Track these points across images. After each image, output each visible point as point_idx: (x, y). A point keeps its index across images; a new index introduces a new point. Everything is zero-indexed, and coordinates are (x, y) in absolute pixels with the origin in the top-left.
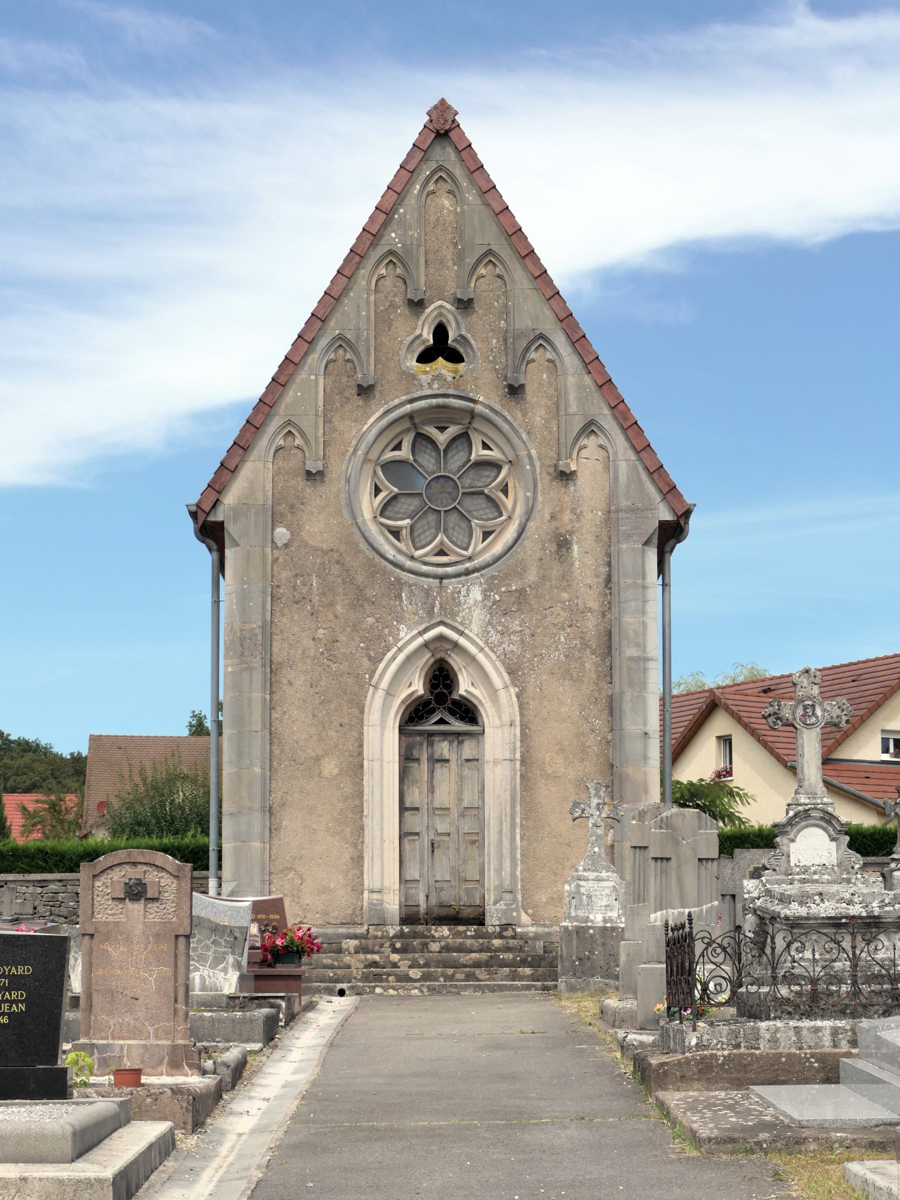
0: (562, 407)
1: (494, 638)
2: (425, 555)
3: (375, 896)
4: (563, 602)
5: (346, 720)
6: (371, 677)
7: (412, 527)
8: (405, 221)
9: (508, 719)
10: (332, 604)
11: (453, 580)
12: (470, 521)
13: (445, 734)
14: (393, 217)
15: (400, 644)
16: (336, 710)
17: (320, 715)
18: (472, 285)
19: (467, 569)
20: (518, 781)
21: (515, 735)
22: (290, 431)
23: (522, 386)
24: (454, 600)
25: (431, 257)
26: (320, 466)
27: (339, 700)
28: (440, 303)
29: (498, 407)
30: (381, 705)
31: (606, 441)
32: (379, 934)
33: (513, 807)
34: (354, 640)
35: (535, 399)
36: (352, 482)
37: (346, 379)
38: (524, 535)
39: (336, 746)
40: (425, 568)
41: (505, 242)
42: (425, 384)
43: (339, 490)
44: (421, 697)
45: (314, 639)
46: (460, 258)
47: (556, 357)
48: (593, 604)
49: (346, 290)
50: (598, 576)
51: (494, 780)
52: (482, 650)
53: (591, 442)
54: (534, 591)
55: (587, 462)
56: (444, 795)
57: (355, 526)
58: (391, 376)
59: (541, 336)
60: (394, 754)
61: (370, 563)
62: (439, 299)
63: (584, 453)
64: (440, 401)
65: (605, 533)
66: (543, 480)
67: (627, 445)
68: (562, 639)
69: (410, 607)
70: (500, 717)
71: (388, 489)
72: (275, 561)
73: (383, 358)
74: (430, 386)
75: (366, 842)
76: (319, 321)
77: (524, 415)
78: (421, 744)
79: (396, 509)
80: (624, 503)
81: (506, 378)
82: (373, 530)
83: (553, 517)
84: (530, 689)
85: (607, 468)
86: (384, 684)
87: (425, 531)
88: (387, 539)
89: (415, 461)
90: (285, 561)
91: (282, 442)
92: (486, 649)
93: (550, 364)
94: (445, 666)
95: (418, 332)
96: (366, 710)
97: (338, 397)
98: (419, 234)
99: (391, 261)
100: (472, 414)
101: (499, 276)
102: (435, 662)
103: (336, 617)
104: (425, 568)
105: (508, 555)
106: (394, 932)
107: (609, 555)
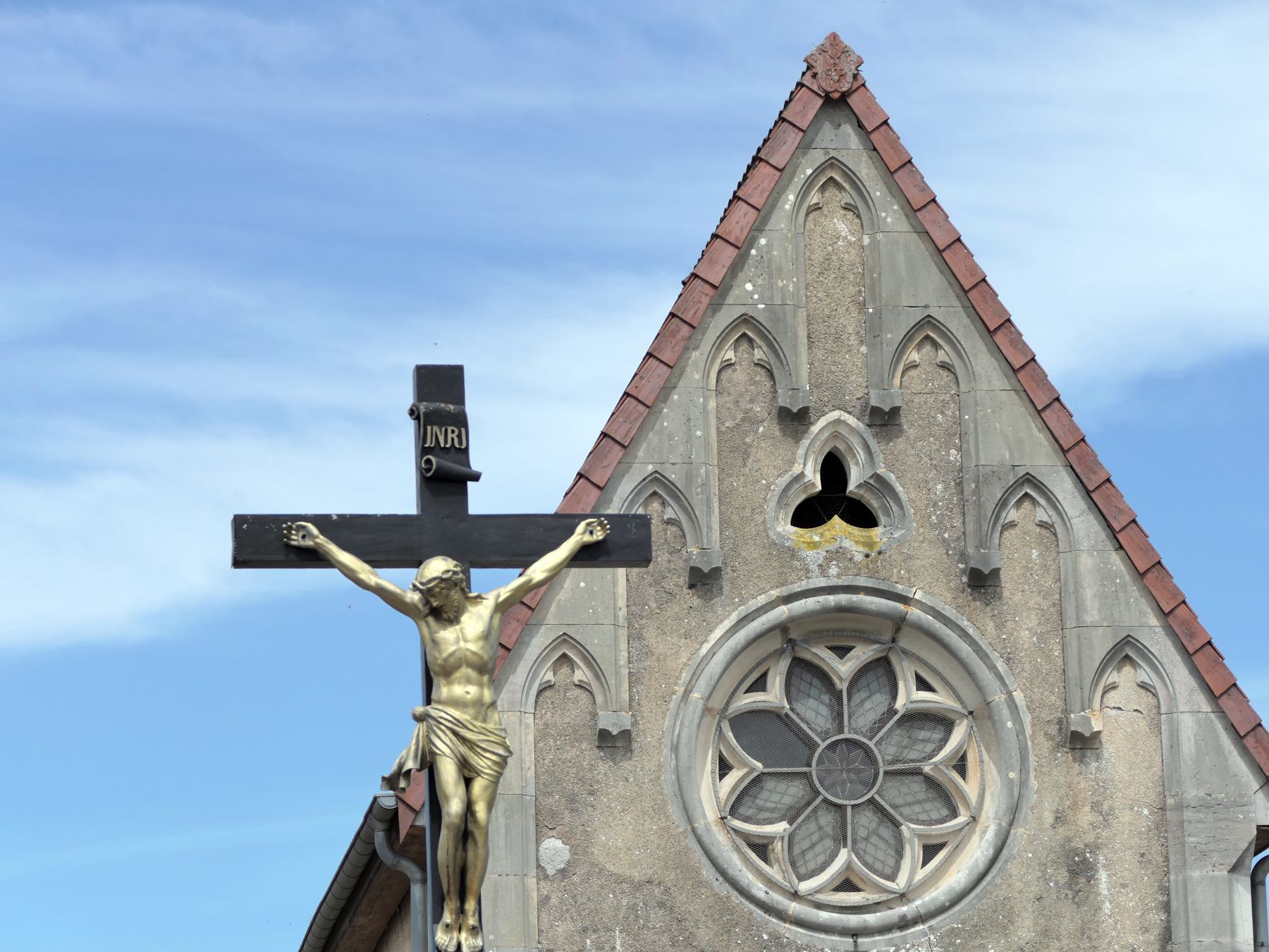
0: (1070, 611)
2: (819, 890)
7: (791, 837)
8: (770, 260)
11: (877, 938)
12: (897, 825)
14: (747, 254)
18: (897, 381)
19: (903, 917)
22: (564, 655)
23: (996, 572)
25: (819, 328)
26: (626, 721)
28: (836, 414)
29: (949, 612)
31: (1153, 675)
35: (1018, 597)
36: (683, 752)
37: (666, 556)
38: (1005, 852)
40: (824, 916)
41: (956, 303)
42: (814, 567)
43: (660, 766)
46: (872, 331)
47: (1055, 518)
49: (666, 391)
50: (1146, 930)
53: (1125, 677)
55: (1117, 714)
57: (691, 835)
58: (751, 552)
59: (1029, 479)
61: (723, 906)
62: (835, 408)
63: (1113, 698)
64: (843, 598)
65: (1156, 848)
66: (1040, 748)
67: (1193, 683)
71: (745, 764)
72: (544, 901)
73: (735, 518)
74: (823, 570)
76: (619, 448)
77: (1000, 626)
79: (760, 802)
80: (1192, 793)
81: (963, 557)
82: (721, 841)
83: (1059, 819)
85: (1156, 727)
87: (813, 846)
88: (746, 860)
89: (792, 709)
90: (562, 902)
91: (550, 676)
93: (1044, 532)
95: (797, 469)
97: (652, 591)
98: (796, 285)
99: (744, 335)
100: (900, 622)
101: (944, 366)
104: (824, 916)
105: (978, 890)
107: (1166, 891)
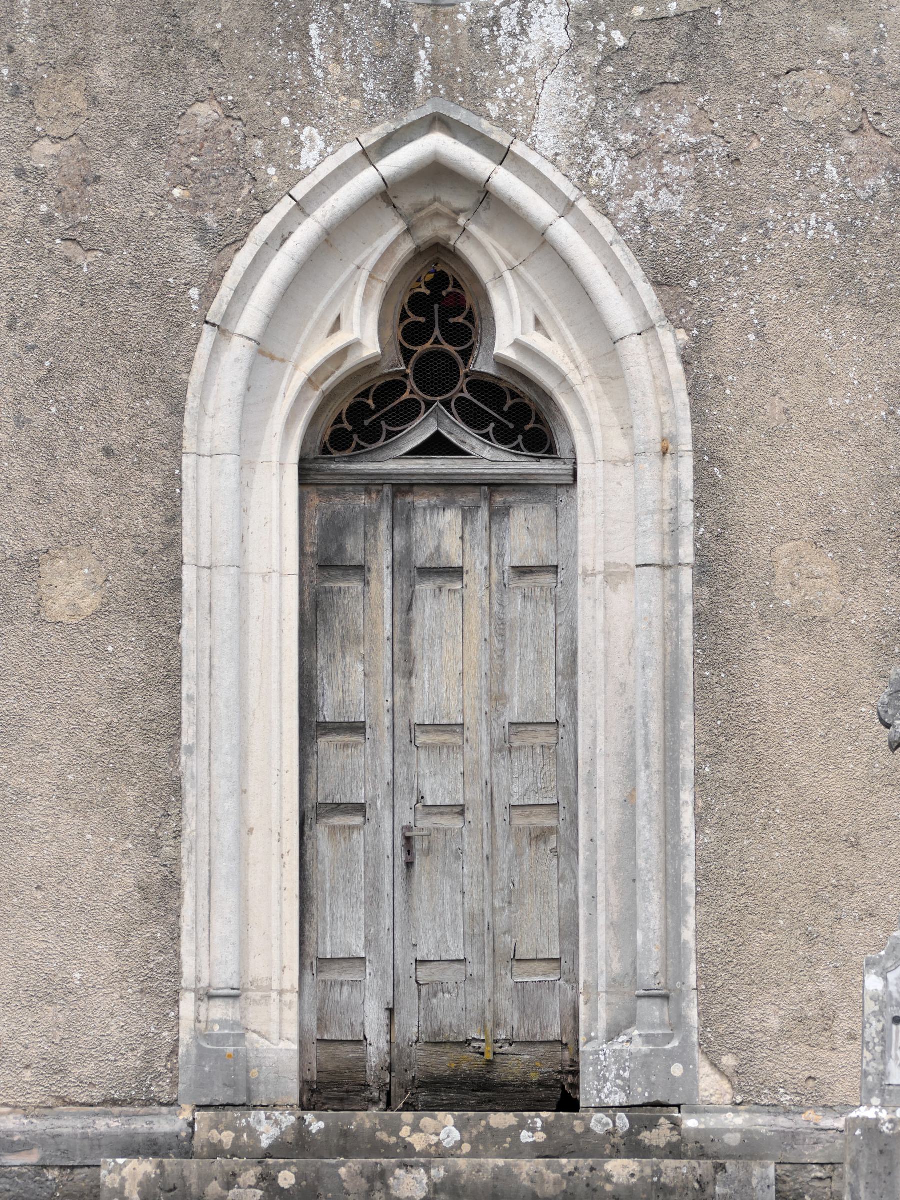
1: (611, 170)
3: (219, 1011)
4: (834, 54)
5: (124, 437)
6: (208, 297)
9: (654, 434)
10: (80, 61)
13: (449, 488)
15: (301, 191)
16: (94, 404)
17: (40, 419)
20: (688, 634)
21: (676, 484)
24: (479, 46)
27: (103, 372)
30: (240, 387)
32: (227, 1138)
33: (671, 717)
34: (151, 176)
39: (93, 520)
44: (370, 366)
45: (20, 173)
51: (608, 634)
52: (568, 208)
54: (738, 19)
56: (445, 684)
60: (282, 551)
68: (832, 172)
69: (335, 70)
70: (627, 430)
75: (189, 831)
78: (372, 518)
84: (726, 334)
86: (250, 320)
92: (584, 205)
94: (450, 269)
96: (192, 404)
102: (419, 254)
103: (94, 101)
106: (275, 1132)
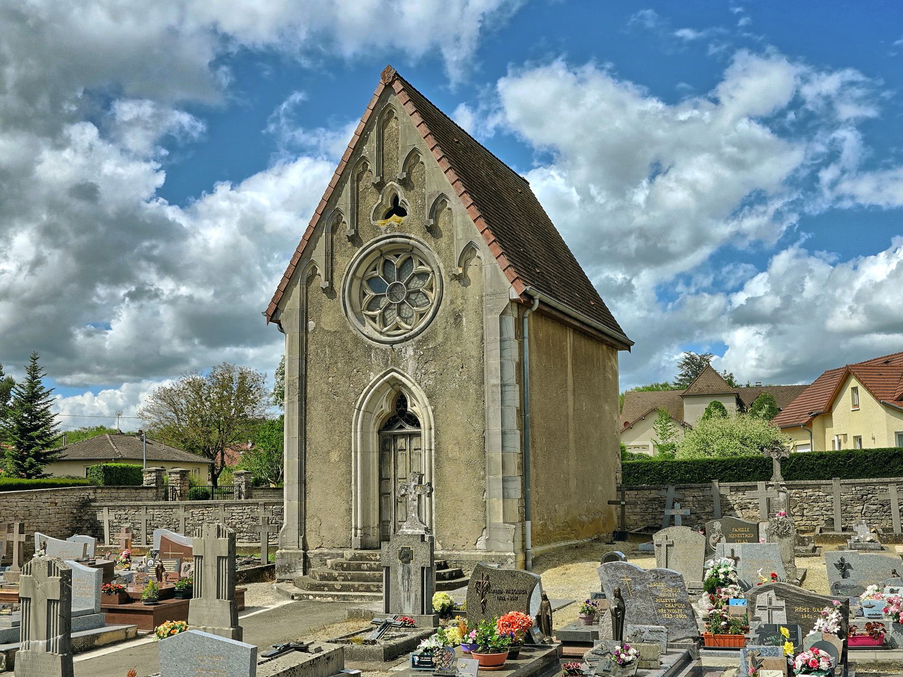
13: (404, 435)
48: (474, 353)
80: (489, 291)
83: (452, 302)
84: (440, 406)
